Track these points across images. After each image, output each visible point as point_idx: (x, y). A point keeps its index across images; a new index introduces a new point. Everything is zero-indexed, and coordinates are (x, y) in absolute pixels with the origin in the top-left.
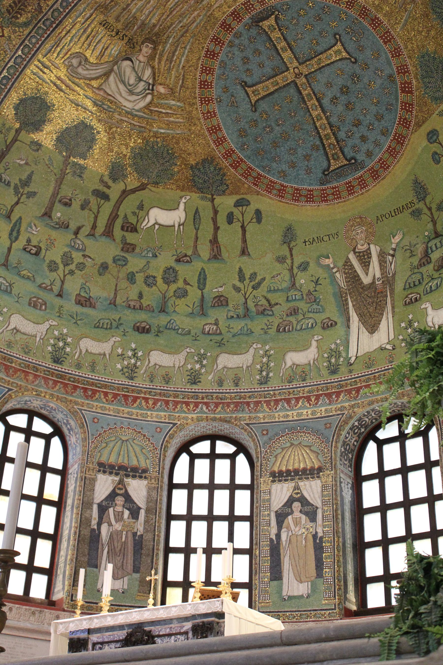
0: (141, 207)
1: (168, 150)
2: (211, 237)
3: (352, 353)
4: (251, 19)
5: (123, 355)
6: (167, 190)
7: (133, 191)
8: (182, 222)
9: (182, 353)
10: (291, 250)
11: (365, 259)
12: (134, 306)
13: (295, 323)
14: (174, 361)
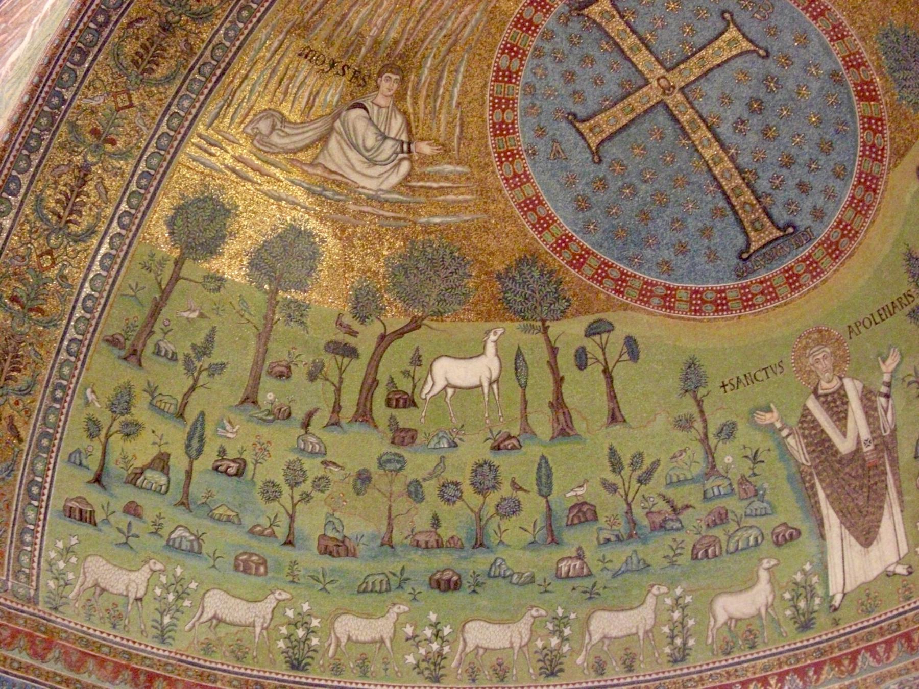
0: (417, 360)
1: (452, 253)
2: (550, 397)
3: (835, 586)
5: (417, 636)
6: (459, 324)
7: (400, 333)
8: (494, 378)
9: (524, 620)
10: (699, 403)
11: (837, 407)
12: (427, 543)
13: (723, 538)
14: (511, 636)
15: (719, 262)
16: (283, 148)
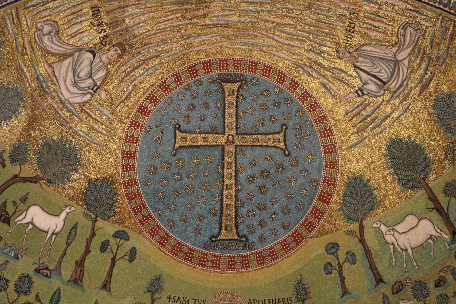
0: (24, 199)
1: (77, 154)
2: (78, 258)
4: (219, 76)
7: (25, 180)
8: (56, 232)
15: (199, 235)
16: (45, 46)
